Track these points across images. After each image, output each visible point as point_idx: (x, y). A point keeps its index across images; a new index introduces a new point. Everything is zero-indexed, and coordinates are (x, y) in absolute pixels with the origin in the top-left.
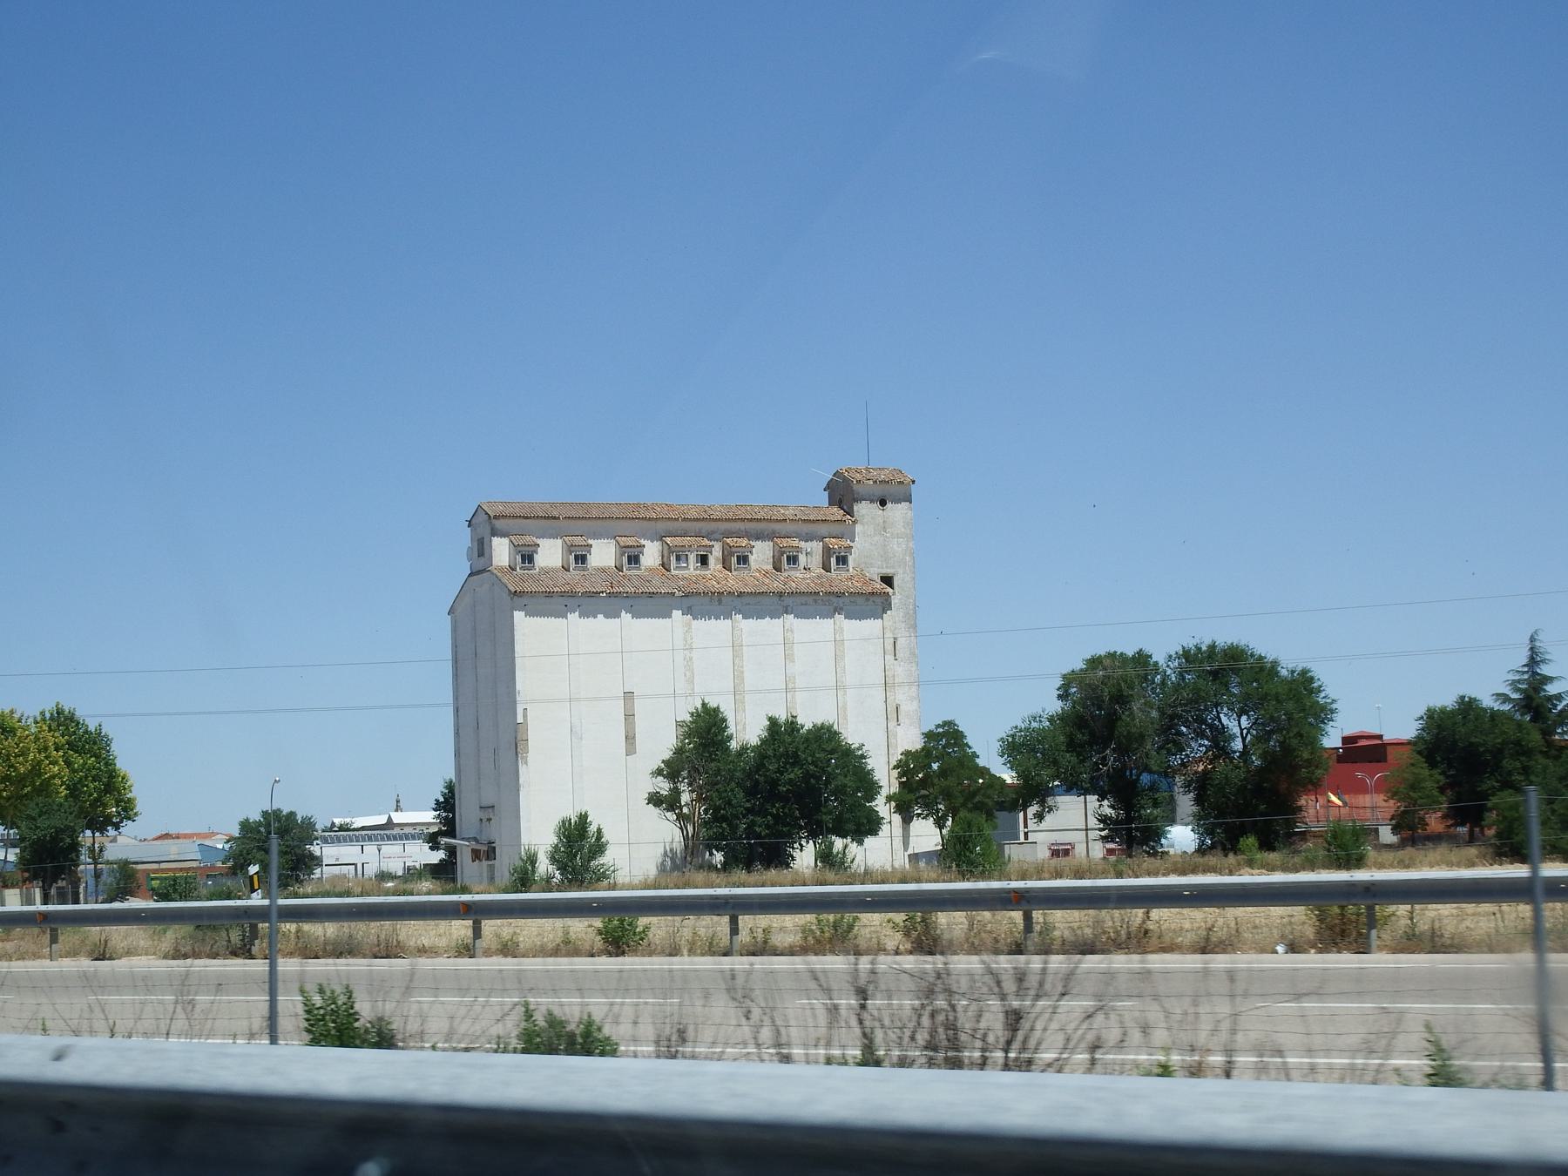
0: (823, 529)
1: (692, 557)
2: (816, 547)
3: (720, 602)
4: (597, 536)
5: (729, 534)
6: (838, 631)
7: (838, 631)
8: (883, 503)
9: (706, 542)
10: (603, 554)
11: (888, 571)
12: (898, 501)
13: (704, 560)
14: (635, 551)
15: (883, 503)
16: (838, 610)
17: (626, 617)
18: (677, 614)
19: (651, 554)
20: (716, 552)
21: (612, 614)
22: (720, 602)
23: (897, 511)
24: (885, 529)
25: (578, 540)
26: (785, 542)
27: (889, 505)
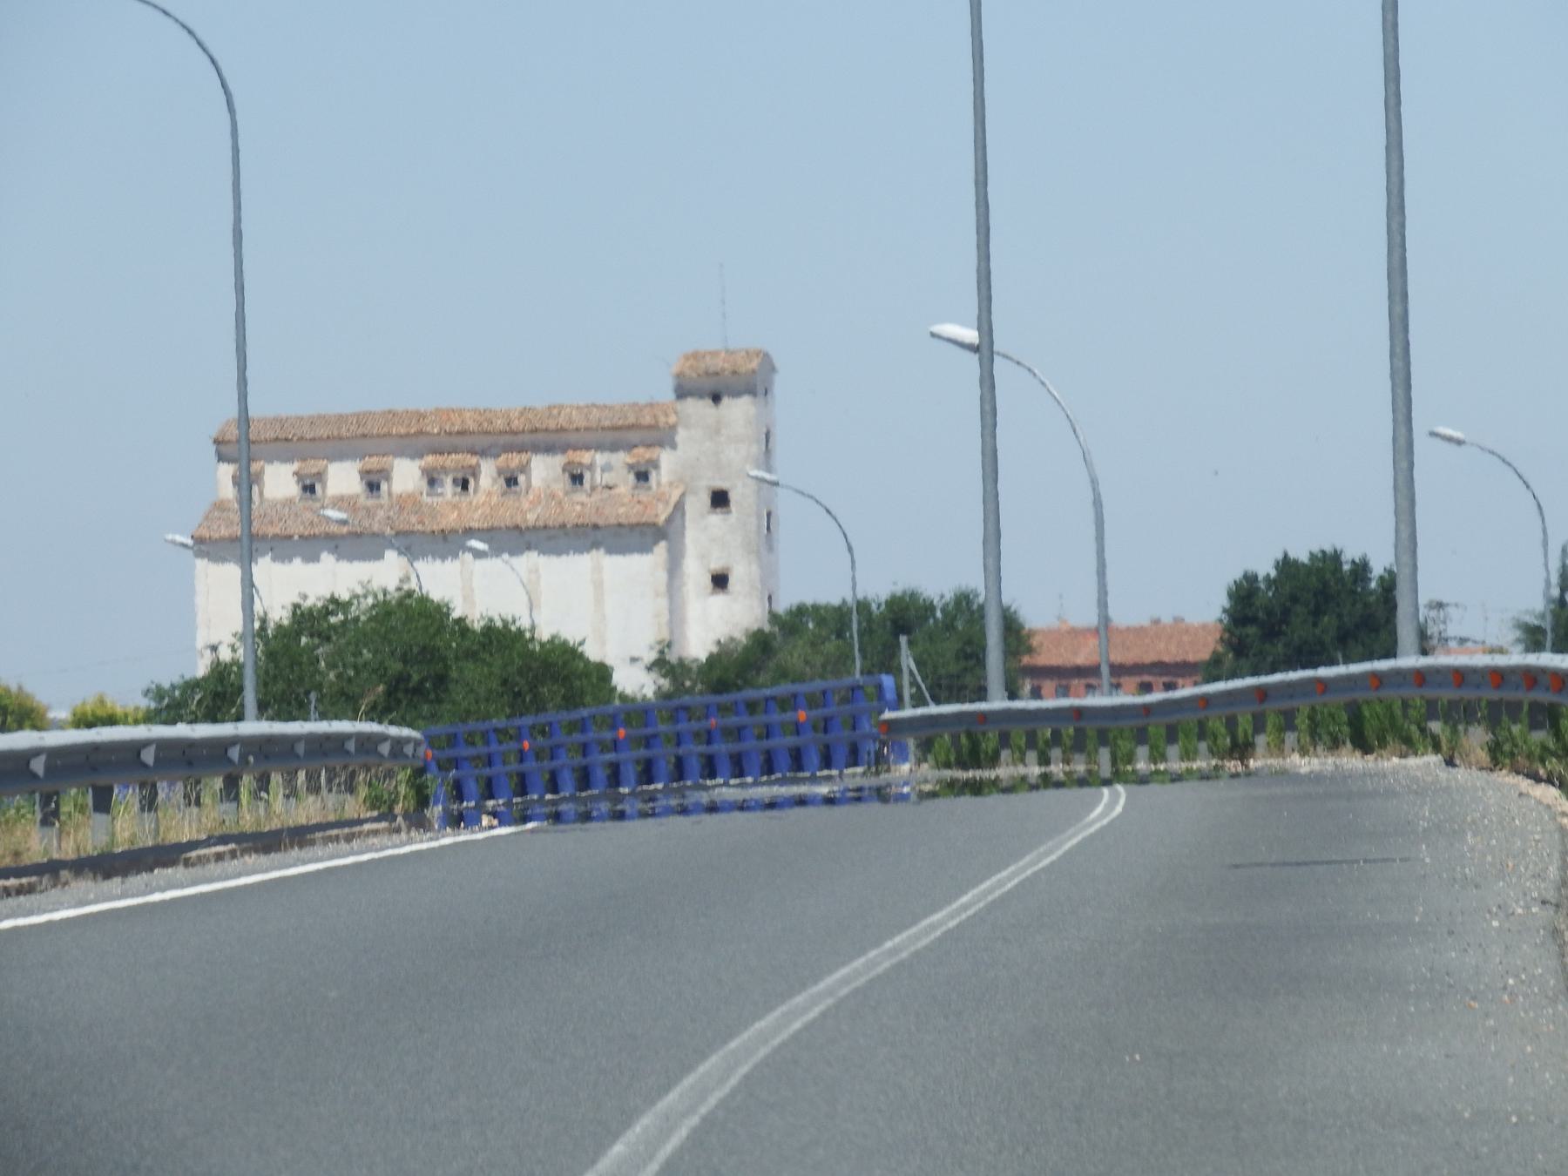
0: (633, 436)
1: (449, 481)
2: (621, 458)
3: (445, 539)
4: (340, 456)
5: (509, 449)
6: (598, 569)
7: (598, 569)
8: (716, 398)
9: (474, 460)
10: (343, 478)
11: (721, 484)
12: (736, 394)
13: (465, 485)
14: (374, 478)
15: (716, 398)
16: (596, 545)
17: (327, 559)
18: (391, 555)
19: (406, 475)
20: (488, 473)
21: (313, 558)
22: (445, 539)
23: (738, 409)
24: (718, 431)
25: (313, 466)
26: (572, 455)
27: (726, 401)
